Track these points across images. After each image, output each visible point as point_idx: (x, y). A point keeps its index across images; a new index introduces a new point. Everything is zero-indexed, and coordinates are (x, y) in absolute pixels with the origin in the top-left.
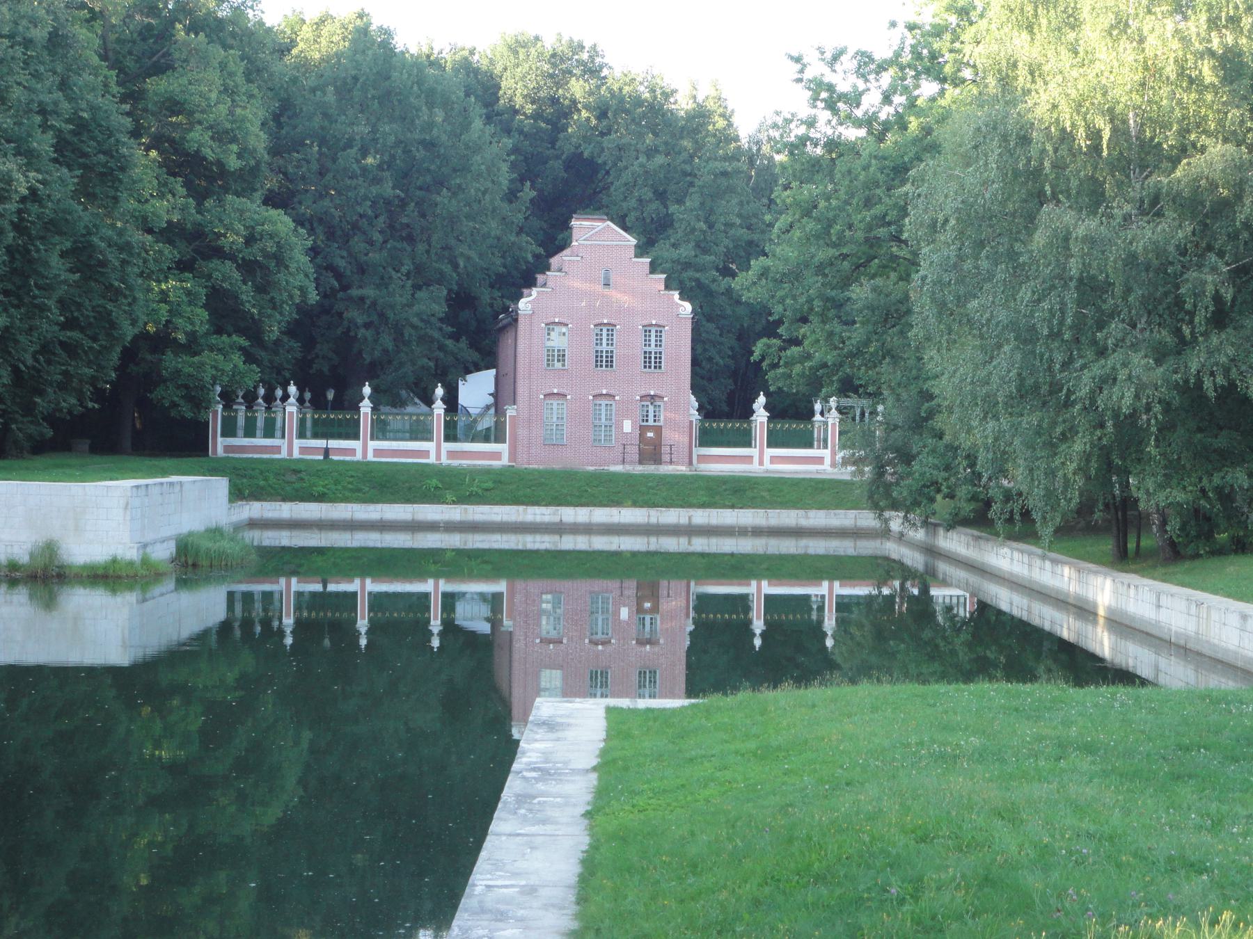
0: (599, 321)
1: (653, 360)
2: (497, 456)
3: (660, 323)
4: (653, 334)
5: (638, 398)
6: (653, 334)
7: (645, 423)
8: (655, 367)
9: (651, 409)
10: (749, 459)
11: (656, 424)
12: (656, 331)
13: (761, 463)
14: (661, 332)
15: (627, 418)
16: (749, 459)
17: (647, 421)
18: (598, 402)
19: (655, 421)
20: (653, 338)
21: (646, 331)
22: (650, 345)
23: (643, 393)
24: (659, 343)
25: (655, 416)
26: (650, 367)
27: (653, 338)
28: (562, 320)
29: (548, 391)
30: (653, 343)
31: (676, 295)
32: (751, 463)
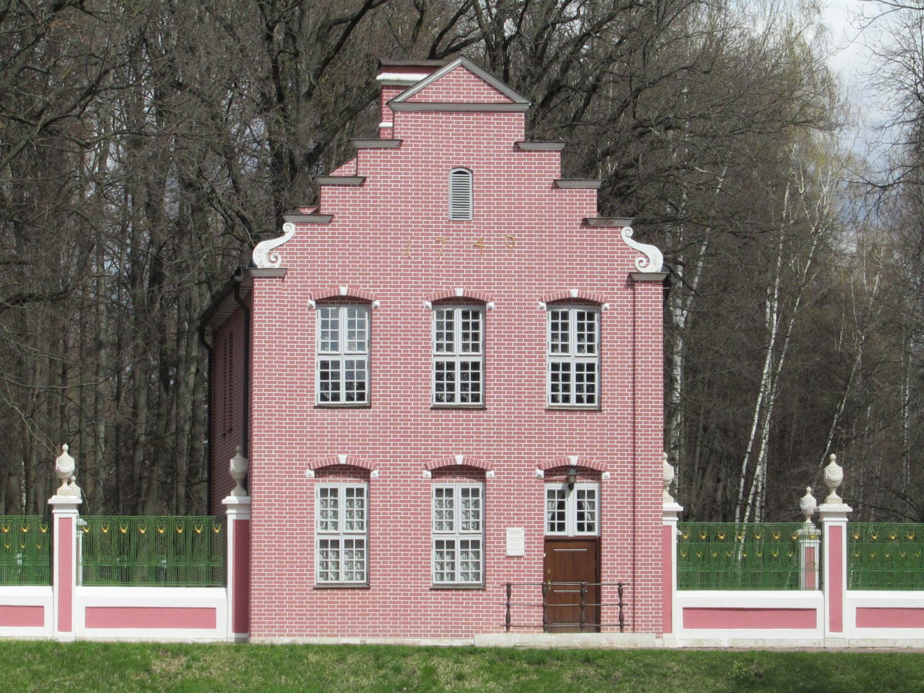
0: (444, 292)
1: (573, 383)
2: (206, 617)
3: (590, 294)
4: (573, 321)
5: (542, 473)
6: (573, 321)
7: (556, 533)
8: (579, 399)
9: (571, 502)
10: (805, 617)
11: (586, 533)
12: (581, 316)
13: (836, 624)
14: (591, 317)
15: (519, 524)
16: (805, 617)
17: (561, 527)
18: (445, 483)
19: (580, 527)
20: (573, 332)
21: (555, 316)
22: (565, 348)
23: (552, 462)
24: (588, 342)
25: (581, 516)
26: (566, 399)
27: (573, 332)
28: (360, 293)
29: (323, 460)
30: (573, 342)
31: (627, 232)
32: (812, 624)
